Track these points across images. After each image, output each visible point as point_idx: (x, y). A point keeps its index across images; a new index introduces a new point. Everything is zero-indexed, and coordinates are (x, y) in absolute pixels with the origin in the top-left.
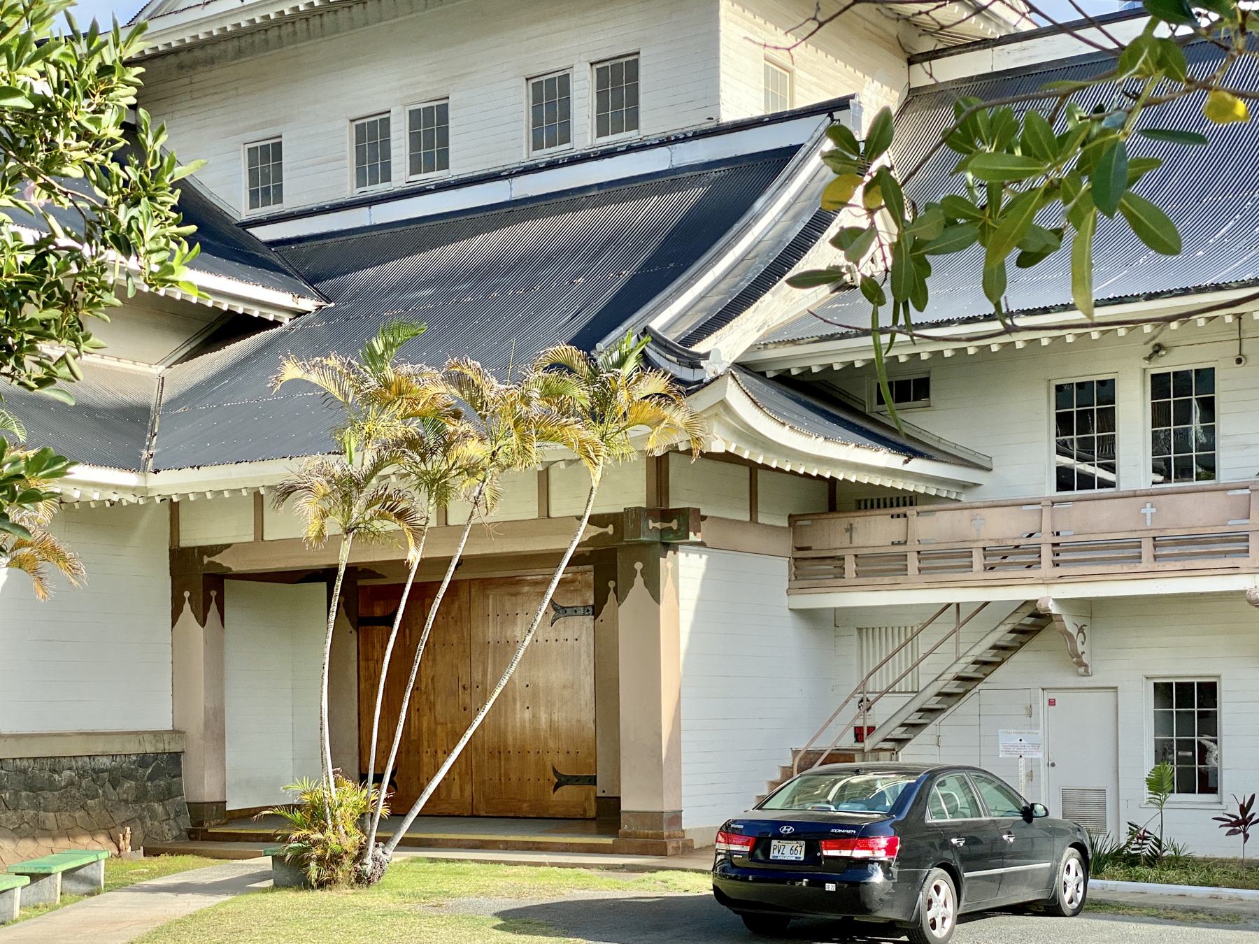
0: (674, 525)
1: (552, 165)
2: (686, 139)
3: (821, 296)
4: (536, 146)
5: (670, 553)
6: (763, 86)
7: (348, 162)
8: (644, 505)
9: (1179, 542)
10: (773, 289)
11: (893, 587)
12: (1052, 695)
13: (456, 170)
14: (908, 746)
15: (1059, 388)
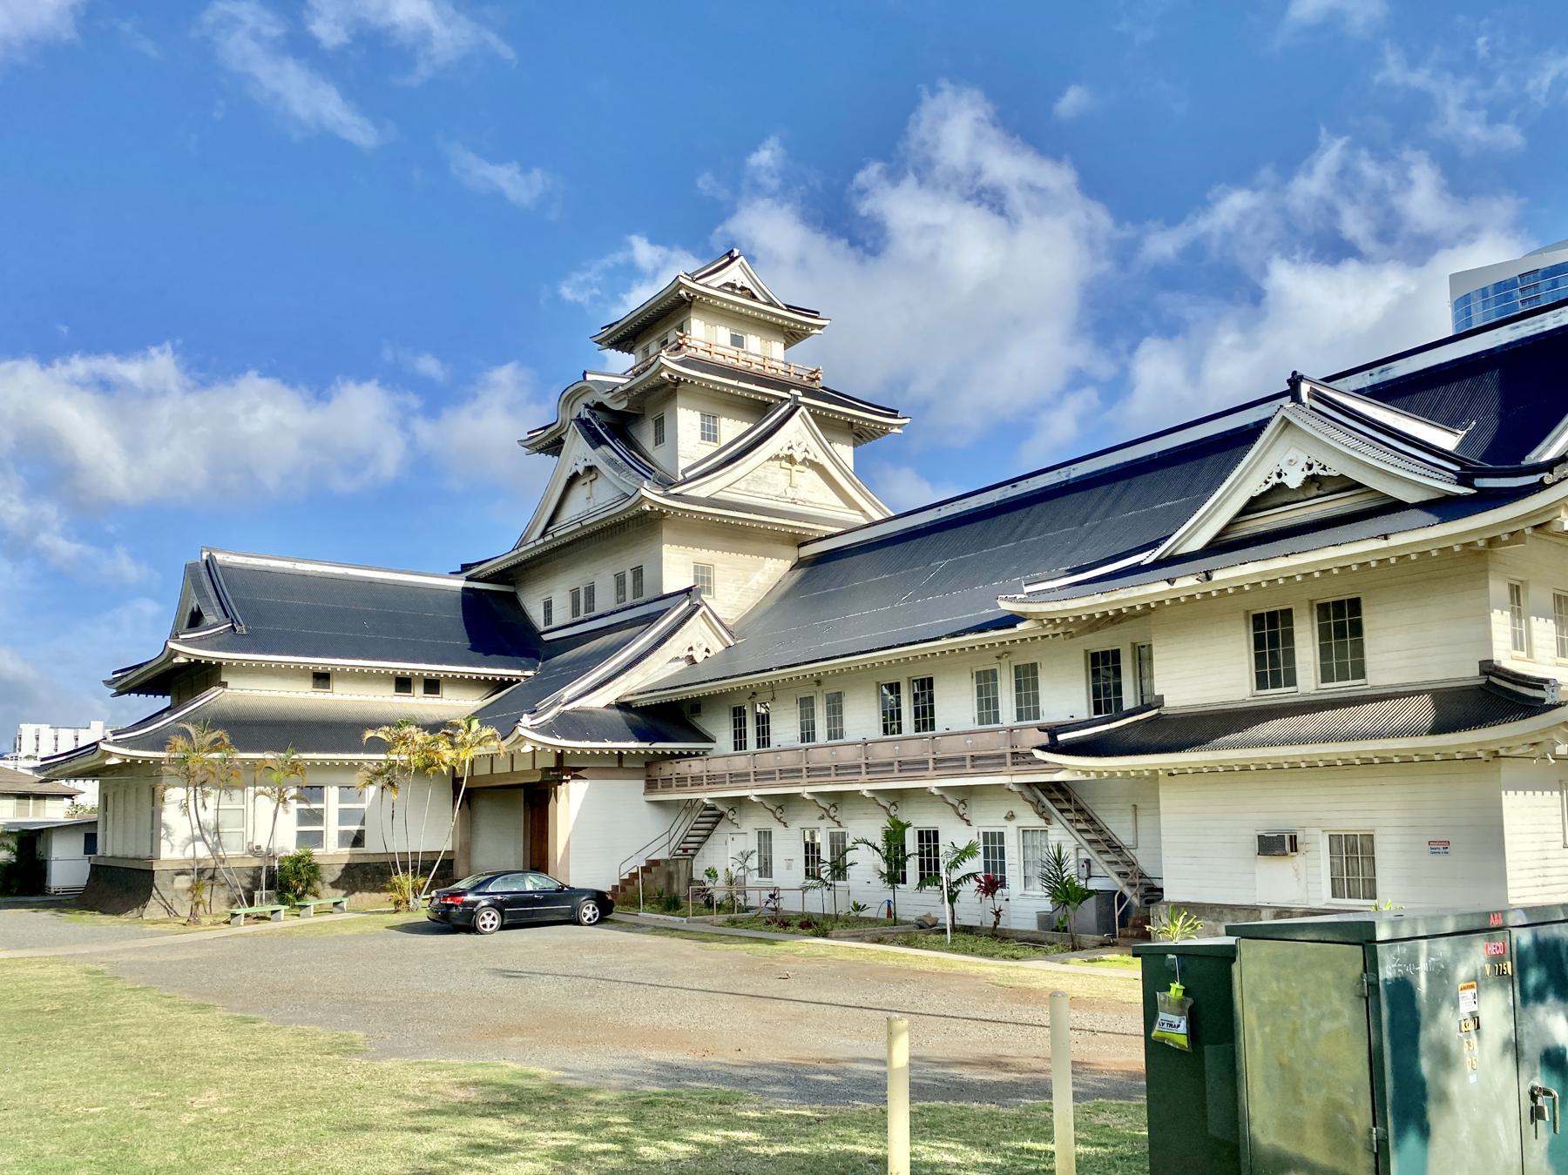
0: (560, 773)
1: (618, 612)
2: (652, 602)
3: (680, 668)
4: (634, 598)
5: (564, 784)
6: (692, 574)
7: (568, 608)
8: (553, 766)
9: (737, 775)
10: (627, 673)
11: (668, 793)
12: (732, 836)
13: (597, 612)
14: (696, 858)
15: (735, 709)
